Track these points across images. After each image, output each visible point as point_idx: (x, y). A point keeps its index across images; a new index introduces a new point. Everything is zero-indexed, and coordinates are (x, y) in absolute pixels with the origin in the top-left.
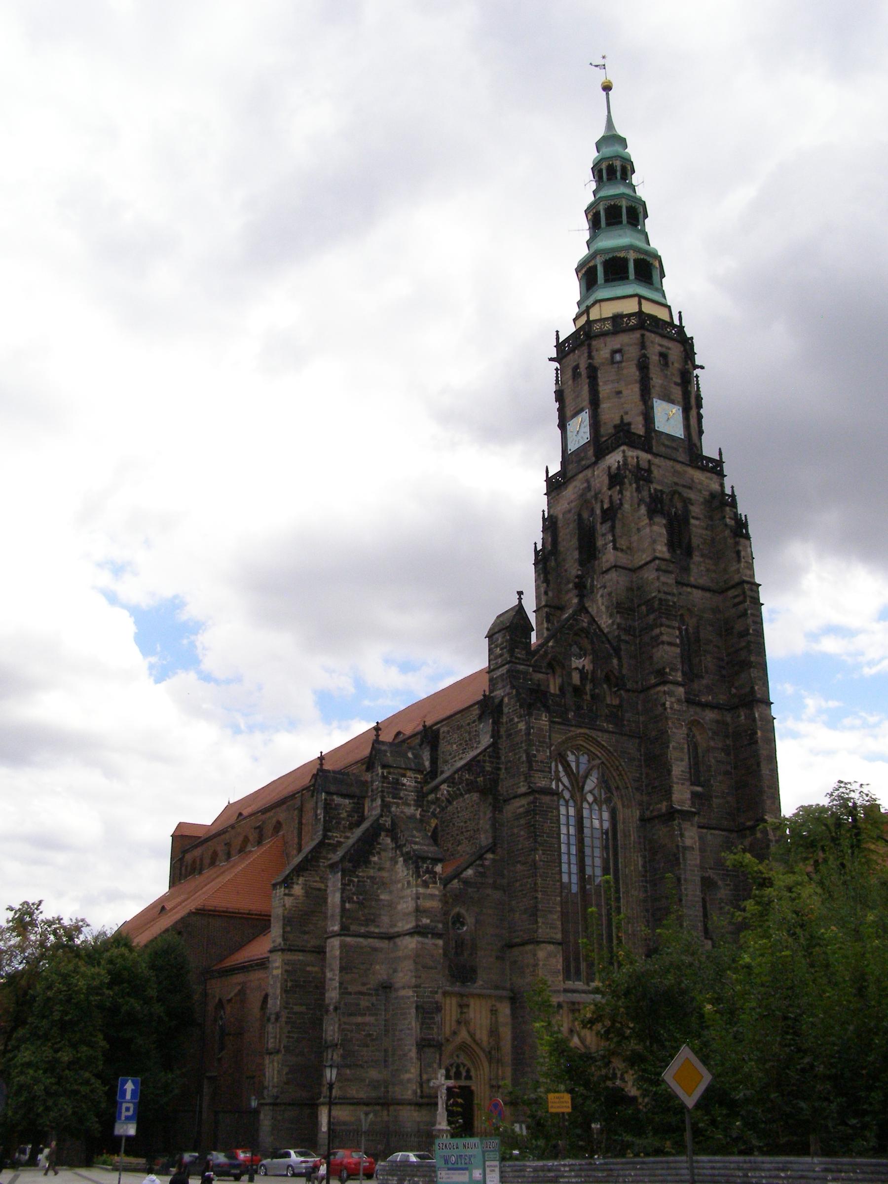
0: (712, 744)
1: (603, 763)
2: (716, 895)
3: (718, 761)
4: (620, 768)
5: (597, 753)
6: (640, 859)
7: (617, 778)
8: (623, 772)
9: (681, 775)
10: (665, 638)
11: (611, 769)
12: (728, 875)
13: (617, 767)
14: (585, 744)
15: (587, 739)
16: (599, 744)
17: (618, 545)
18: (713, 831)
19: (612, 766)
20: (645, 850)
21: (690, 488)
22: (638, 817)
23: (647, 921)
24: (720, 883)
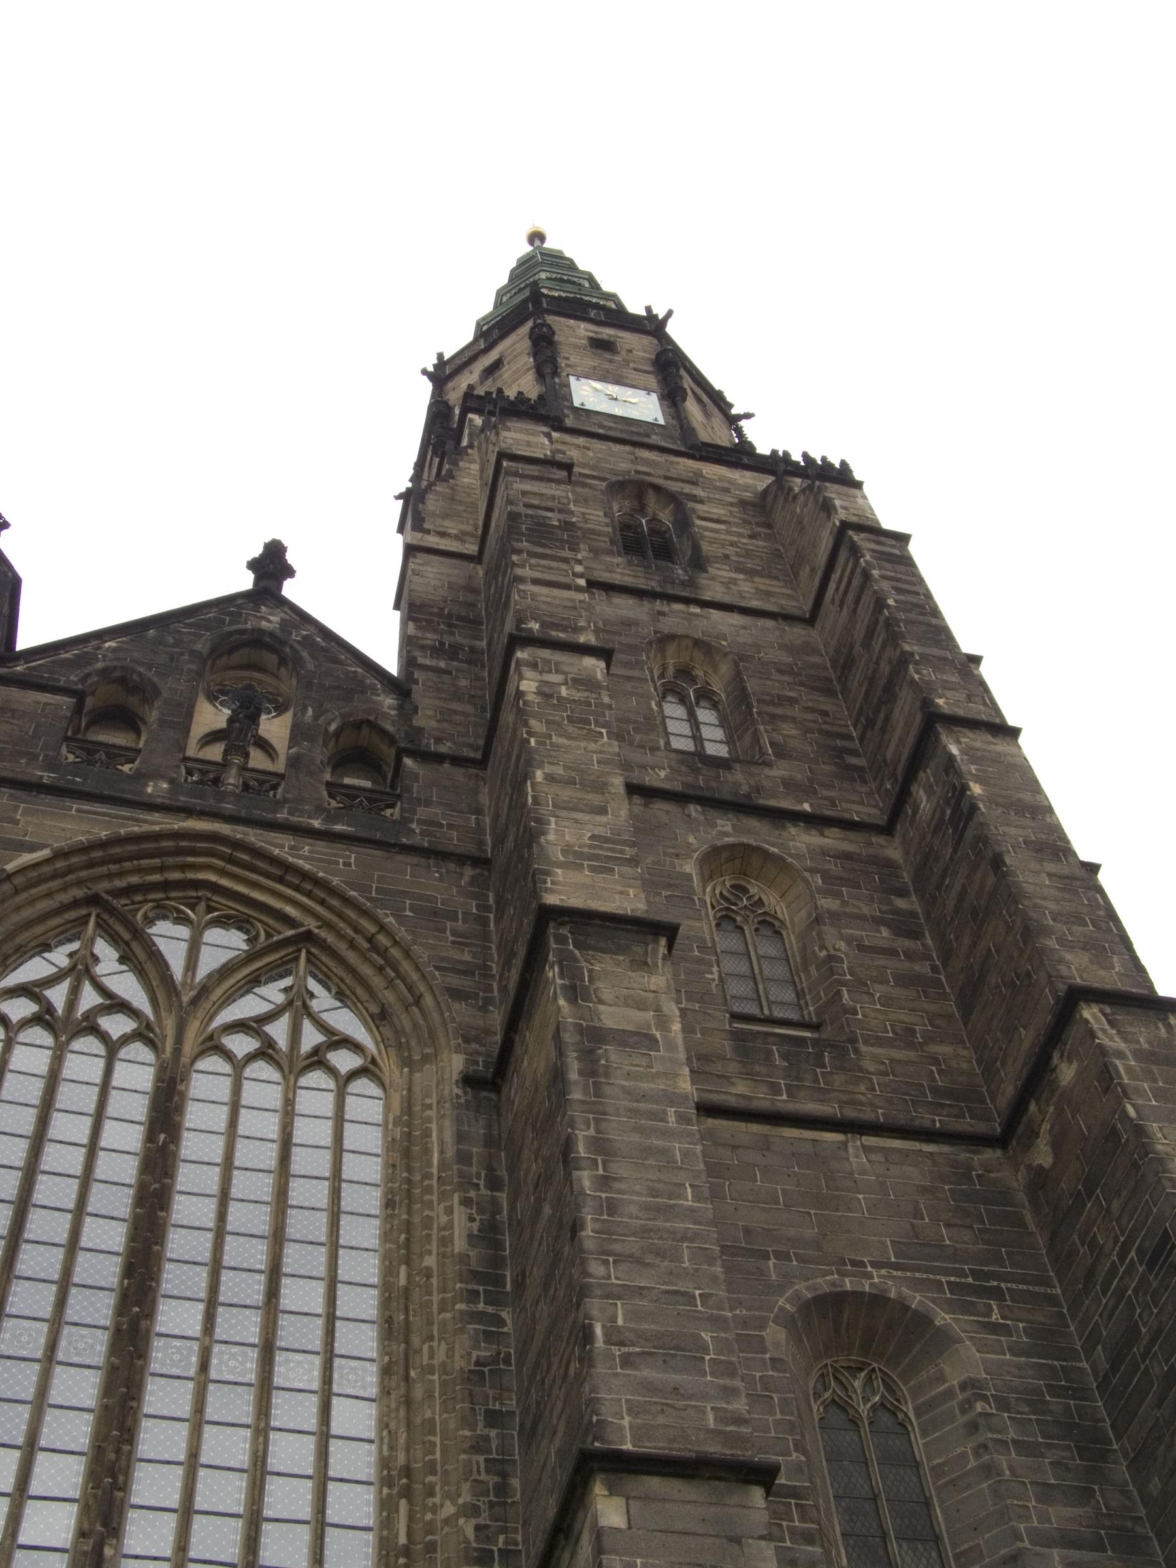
0: (828, 903)
1: (308, 937)
2: (941, 1378)
3: (861, 948)
4: (382, 939)
5: (290, 910)
6: (460, 1214)
7: (377, 981)
8: (395, 953)
9: (590, 846)
10: (525, 572)
11: (351, 957)
12: (997, 1294)
13: (370, 940)
14: (225, 882)
15: (231, 860)
16: (284, 871)
17: (426, 526)
18: (871, 1141)
19: (352, 945)
20: (494, 1183)
21: (695, 484)
22: (455, 1077)
23: (500, 1467)
24: (943, 1318)
